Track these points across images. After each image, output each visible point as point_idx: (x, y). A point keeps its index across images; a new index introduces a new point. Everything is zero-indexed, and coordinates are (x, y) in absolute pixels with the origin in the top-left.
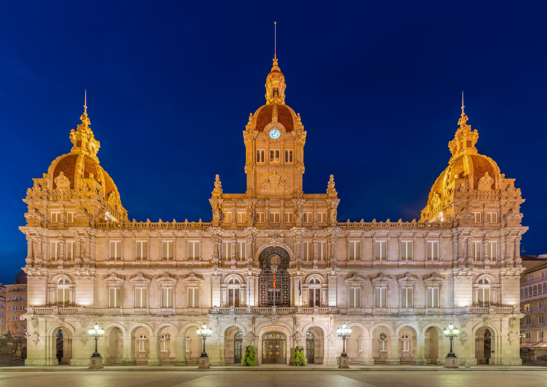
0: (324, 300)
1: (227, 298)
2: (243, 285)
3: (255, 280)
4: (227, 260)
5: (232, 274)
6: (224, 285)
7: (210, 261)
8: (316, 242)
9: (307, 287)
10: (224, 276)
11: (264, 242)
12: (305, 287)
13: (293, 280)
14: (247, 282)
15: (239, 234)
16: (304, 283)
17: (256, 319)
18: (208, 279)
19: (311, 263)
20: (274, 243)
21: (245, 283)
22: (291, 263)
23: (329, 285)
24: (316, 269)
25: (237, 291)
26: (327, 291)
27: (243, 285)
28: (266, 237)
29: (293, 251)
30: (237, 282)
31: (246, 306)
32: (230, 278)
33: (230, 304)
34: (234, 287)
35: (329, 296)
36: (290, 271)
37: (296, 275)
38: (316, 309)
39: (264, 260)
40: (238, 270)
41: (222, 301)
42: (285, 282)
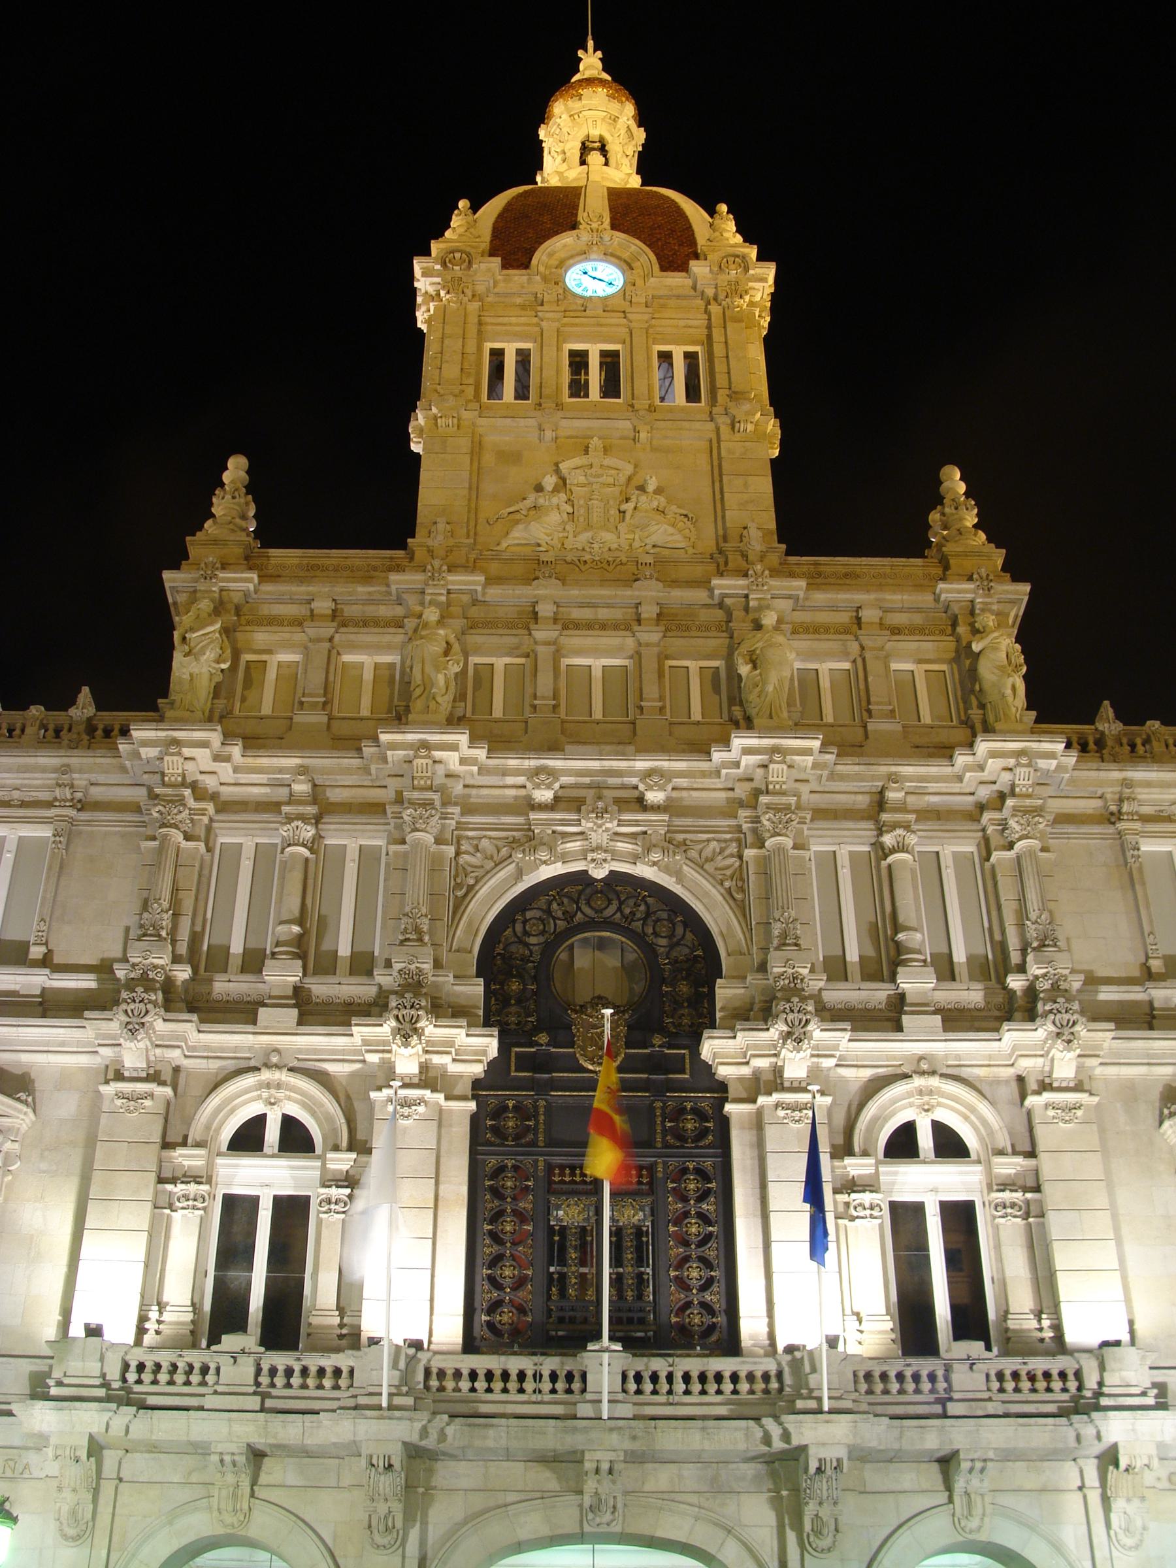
0: (1022, 1300)
1: (199, 1273)
2: (342, 1162)
3: (441, 1119)
4: (235, 963)
5: (270, 1069)
6: (186, 1158)
7: (103, 969)
8: (901, 848)
9: (870, 1185)
10: (196, 1091)
11: (528, 840)
12: (850, 1186)
13: (758, 1123)
14: (379, 1142)
15: (341, 773)
16: (844, 1149)
17: (447, 1474)
18: (64, 1107)
19: (877, 995)
20: (599, 849)
21: (360, 1146)
22: (725, 992)
23: (1047, 1165)
24: (920, 1041)
25: (292, 1213)
26: (1034, 1214)
27: (342, 1162)
28: (542, 807)
29: (742, 909)
30: (295, 1138)
31: (352, 1339)
32: (241, 1103)
33: (226, 1314)
34: (266, 1177)
35: (1062, 1259)
36: (725, 1052)
37: (775, 1081)
38: (966, 1365)
39: (521, 973)
40: (315, 1042)
41: (152, 1297)
42: (688, 1145)
